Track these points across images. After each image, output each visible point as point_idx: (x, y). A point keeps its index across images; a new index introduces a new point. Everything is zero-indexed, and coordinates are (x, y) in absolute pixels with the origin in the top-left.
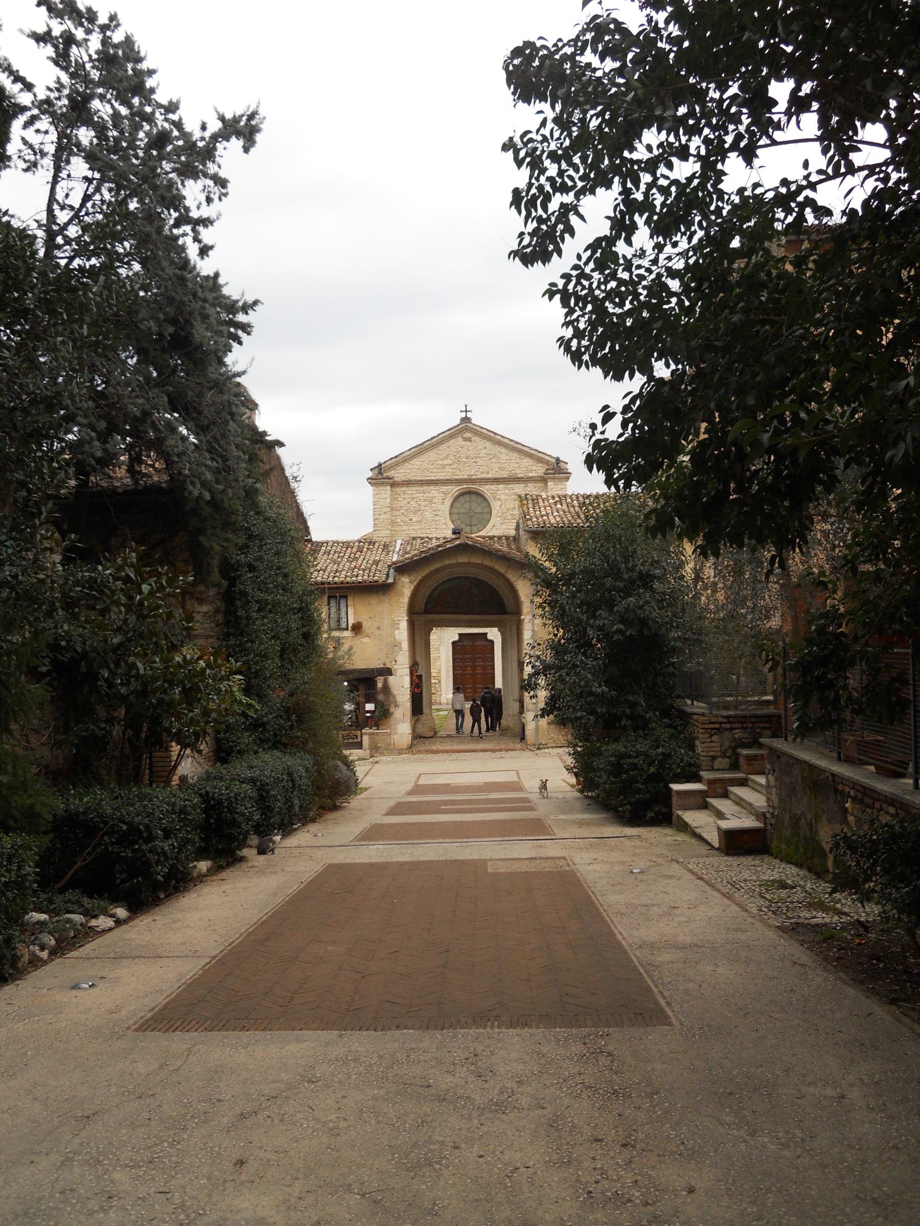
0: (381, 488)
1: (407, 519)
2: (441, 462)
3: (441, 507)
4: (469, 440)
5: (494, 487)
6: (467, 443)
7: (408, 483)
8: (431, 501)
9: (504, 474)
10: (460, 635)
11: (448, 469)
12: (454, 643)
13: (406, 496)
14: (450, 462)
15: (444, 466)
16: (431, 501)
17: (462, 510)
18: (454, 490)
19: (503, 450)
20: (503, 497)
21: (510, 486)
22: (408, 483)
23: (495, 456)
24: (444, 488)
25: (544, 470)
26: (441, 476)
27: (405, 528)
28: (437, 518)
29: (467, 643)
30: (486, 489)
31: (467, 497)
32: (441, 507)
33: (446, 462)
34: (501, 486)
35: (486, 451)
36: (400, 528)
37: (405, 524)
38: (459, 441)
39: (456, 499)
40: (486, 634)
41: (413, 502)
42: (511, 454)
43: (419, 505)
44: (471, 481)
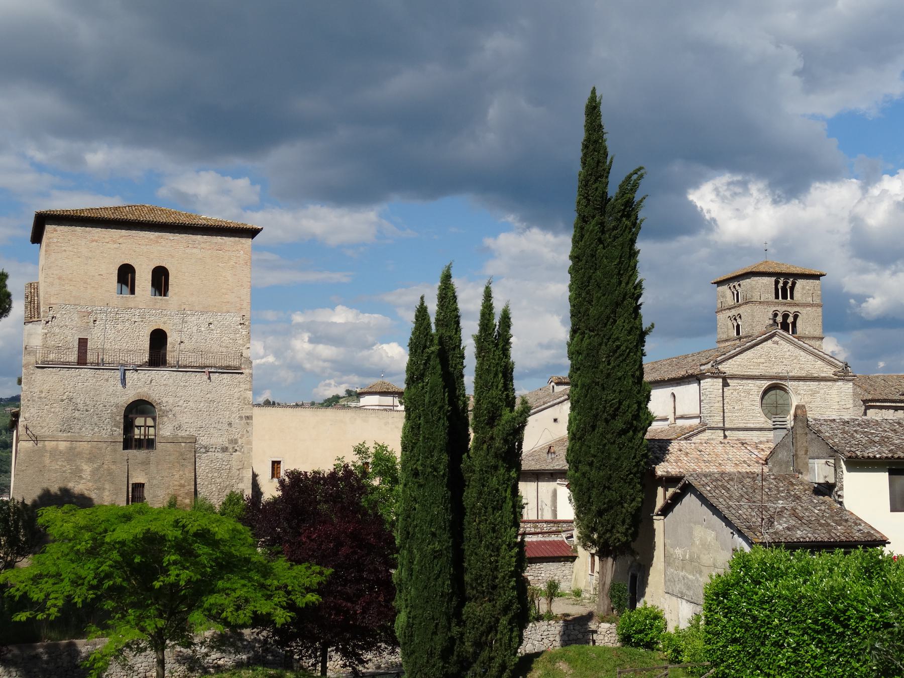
2: (755, 360)
5: (796, 383)
6: (776, 346)
7: (733, 377)
9: (803, 374)
14: (763, 360)
15: (759, 364)
18: (766, 384)
19: (802, 353)
20: (802, 392)
22: (733, 377)
23: (796, 357)
24: (758, 382)
25: (832, 372)
26: (756, 373)
27: (730, 414)
30: (790, 385)
31: (773, 392)
33: (759, 361)
34: (801, 383)
35: (788, 353)
38: (770, 342)
39: (766, 392)
41: (735, 393)
44: (781, 378)
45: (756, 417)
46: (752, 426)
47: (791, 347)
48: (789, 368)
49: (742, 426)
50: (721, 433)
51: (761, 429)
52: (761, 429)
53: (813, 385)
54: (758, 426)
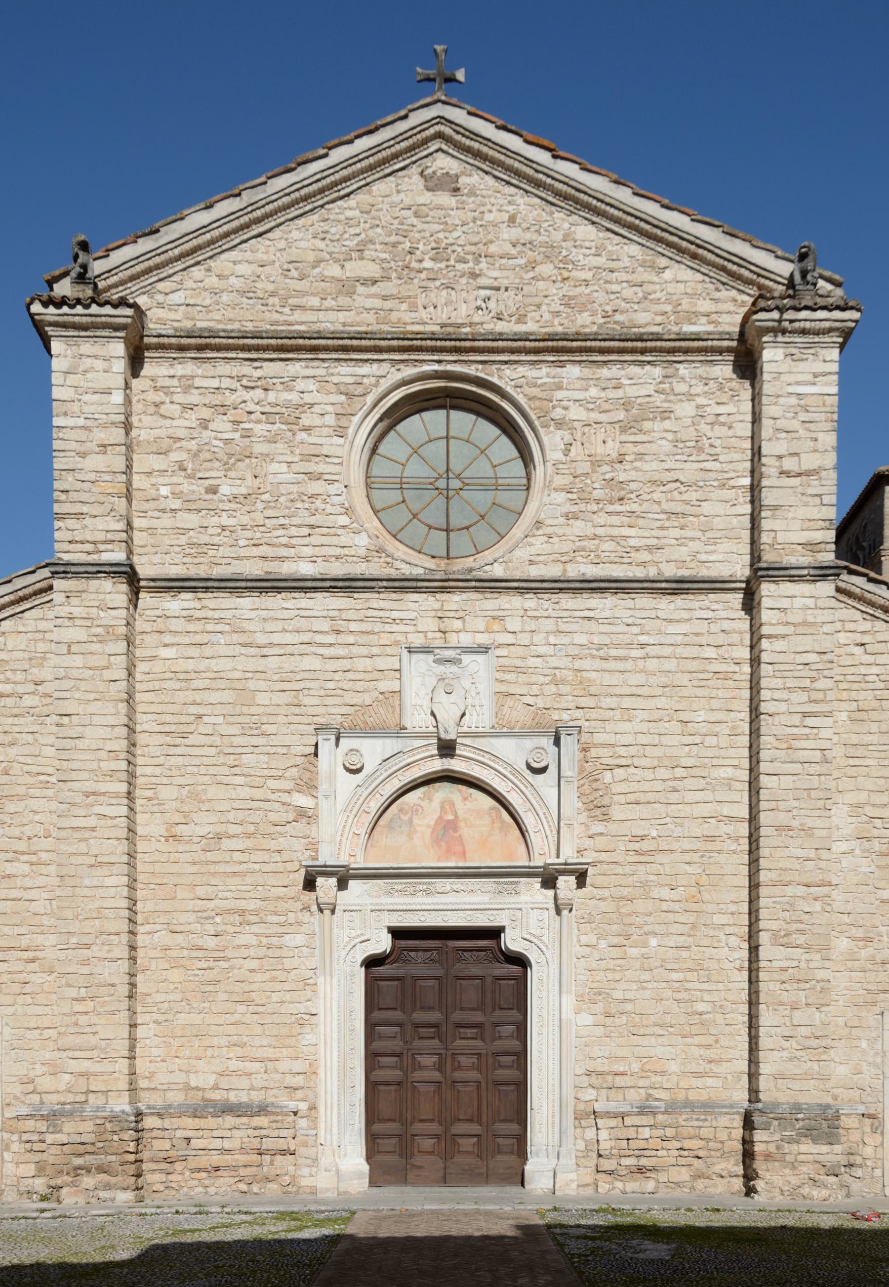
0: (86, 347)
1: (199, 488)
3: (332, 445)
4: (450, 184)
5: (543, 373)
6: (445, 199)
8: (293, 422)
10: (397, 933)
11: (364, 298)
12: (372, 963)
13: (194, 398)
16: (293, 422)
17: (416, 470)
19: (586, 232)
21: (605, 372)
23: (550, 252)
26: (331, 321)
28: (316, 487)
29: (420, 963)
30: (514, 378)
32: (332, 445)
34: (573, 371)
35: (515, 233)
36: (166, 521)
37: (190, 505)
39: (396, 415)
40: (495, 933)
42: (613, 244)
43: (247, 435)
45: (332, 530)
46: (306, 569)
47: (527, 205)
48: (509, 301)
49: (254, 569)
50: (115, 592)
51: (347, 585)
52: (347, 585)
53: (640, 380)
54: (338, 569)
